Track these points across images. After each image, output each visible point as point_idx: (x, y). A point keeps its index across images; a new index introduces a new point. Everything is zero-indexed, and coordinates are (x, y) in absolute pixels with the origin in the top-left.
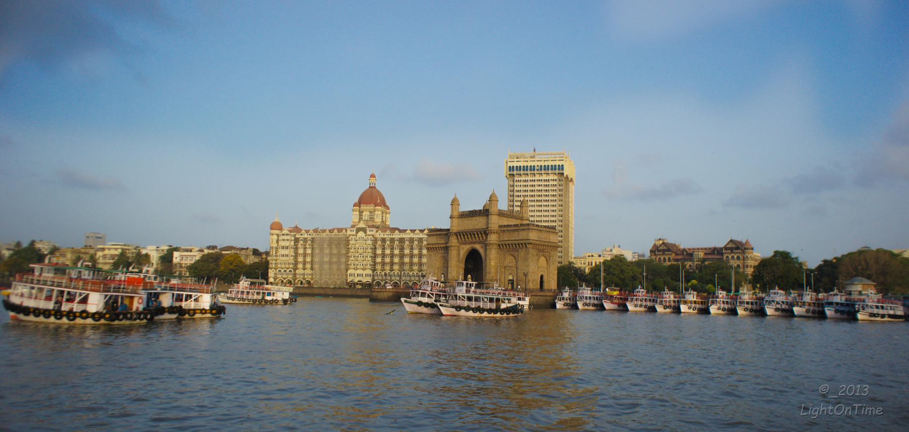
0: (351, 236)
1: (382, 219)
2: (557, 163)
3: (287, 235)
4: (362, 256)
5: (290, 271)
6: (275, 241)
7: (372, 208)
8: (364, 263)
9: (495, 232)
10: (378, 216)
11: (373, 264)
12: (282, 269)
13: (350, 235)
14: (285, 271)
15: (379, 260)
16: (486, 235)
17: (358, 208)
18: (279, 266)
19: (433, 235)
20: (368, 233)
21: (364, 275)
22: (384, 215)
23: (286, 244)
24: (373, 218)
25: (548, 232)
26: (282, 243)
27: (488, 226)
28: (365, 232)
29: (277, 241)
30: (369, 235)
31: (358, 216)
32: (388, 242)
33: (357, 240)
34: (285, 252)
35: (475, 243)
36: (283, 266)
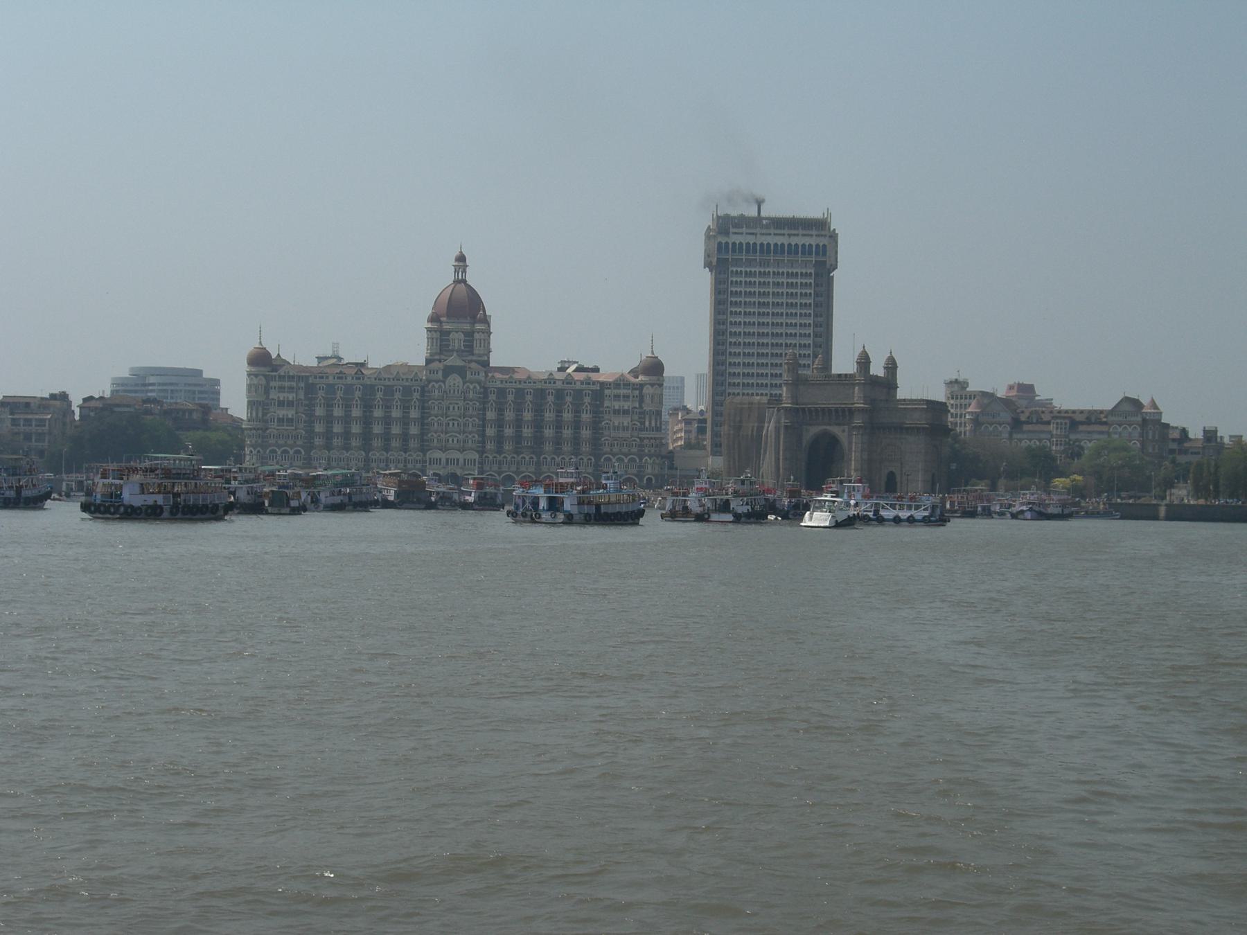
0: (434, 383)
2: (813, 241)
4: (456, 423)
5: (298, 452)
7: (467, 327)
10: (482, 341)
11: (480, 439)
12: (279, 446)
13: (429, 381)
14: (285, 452)
18: (272, 441)
20: (469, 376)
21: (461, 461)
23: (291, 396)
24: (471, 347)
26: (274, 395)
28: (463, 376)
29: (267, 390)
33: (445, 392)
34: (290, 413)
35: (830, 425)
36: (281, 442)
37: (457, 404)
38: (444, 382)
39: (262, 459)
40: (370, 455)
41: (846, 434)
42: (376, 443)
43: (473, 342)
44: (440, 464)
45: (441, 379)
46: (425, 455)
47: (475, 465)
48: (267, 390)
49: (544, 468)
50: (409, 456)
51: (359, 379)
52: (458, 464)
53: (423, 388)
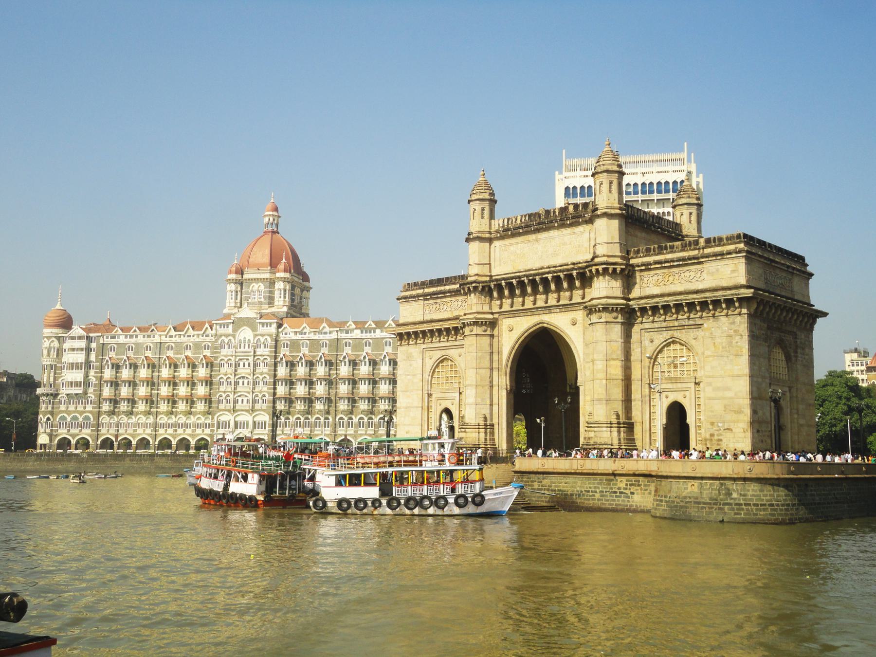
0: (224, 338)
1: (292, 300)
3: (80, 338)
4: (246, 381)
6: (53, 354)
7: (268, 276)
8: (250, 397)
9: (619, 268)
12: (69, 415)
15: (281, 390)
16: (591, 279)
17: (239, 276)
19: (416, 297)
22: (297, 291)
23: (80, 358)
25: (788, 267)
26: (68, 358)
27: (594, 253)
28: (254, 329)
30: (262, 335)
31: (239, 293)
32: (305, 350)
34: (78, 376)
35: (548, 309)
37: (248, 359)
38: (234, 336)
39: (52, 427)
40: (158, 420)
41: (579, 327)
42: (164, 407)
43: (274, 294)
44: (229, 428)
45: (231, 333)
46: (213, 419)
47: (265, 428)
48: (60, 352)
49: (341, 431)
50: (198, 419)
51: (149, 336)
52: (247, 428)
53: (213, 343)
